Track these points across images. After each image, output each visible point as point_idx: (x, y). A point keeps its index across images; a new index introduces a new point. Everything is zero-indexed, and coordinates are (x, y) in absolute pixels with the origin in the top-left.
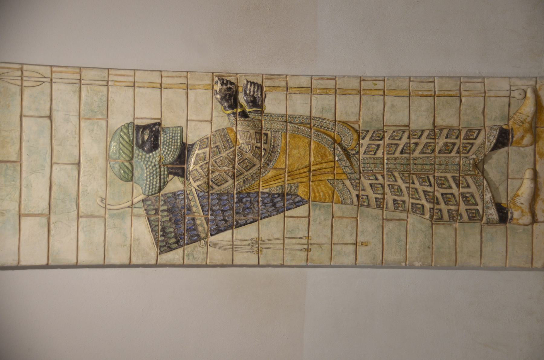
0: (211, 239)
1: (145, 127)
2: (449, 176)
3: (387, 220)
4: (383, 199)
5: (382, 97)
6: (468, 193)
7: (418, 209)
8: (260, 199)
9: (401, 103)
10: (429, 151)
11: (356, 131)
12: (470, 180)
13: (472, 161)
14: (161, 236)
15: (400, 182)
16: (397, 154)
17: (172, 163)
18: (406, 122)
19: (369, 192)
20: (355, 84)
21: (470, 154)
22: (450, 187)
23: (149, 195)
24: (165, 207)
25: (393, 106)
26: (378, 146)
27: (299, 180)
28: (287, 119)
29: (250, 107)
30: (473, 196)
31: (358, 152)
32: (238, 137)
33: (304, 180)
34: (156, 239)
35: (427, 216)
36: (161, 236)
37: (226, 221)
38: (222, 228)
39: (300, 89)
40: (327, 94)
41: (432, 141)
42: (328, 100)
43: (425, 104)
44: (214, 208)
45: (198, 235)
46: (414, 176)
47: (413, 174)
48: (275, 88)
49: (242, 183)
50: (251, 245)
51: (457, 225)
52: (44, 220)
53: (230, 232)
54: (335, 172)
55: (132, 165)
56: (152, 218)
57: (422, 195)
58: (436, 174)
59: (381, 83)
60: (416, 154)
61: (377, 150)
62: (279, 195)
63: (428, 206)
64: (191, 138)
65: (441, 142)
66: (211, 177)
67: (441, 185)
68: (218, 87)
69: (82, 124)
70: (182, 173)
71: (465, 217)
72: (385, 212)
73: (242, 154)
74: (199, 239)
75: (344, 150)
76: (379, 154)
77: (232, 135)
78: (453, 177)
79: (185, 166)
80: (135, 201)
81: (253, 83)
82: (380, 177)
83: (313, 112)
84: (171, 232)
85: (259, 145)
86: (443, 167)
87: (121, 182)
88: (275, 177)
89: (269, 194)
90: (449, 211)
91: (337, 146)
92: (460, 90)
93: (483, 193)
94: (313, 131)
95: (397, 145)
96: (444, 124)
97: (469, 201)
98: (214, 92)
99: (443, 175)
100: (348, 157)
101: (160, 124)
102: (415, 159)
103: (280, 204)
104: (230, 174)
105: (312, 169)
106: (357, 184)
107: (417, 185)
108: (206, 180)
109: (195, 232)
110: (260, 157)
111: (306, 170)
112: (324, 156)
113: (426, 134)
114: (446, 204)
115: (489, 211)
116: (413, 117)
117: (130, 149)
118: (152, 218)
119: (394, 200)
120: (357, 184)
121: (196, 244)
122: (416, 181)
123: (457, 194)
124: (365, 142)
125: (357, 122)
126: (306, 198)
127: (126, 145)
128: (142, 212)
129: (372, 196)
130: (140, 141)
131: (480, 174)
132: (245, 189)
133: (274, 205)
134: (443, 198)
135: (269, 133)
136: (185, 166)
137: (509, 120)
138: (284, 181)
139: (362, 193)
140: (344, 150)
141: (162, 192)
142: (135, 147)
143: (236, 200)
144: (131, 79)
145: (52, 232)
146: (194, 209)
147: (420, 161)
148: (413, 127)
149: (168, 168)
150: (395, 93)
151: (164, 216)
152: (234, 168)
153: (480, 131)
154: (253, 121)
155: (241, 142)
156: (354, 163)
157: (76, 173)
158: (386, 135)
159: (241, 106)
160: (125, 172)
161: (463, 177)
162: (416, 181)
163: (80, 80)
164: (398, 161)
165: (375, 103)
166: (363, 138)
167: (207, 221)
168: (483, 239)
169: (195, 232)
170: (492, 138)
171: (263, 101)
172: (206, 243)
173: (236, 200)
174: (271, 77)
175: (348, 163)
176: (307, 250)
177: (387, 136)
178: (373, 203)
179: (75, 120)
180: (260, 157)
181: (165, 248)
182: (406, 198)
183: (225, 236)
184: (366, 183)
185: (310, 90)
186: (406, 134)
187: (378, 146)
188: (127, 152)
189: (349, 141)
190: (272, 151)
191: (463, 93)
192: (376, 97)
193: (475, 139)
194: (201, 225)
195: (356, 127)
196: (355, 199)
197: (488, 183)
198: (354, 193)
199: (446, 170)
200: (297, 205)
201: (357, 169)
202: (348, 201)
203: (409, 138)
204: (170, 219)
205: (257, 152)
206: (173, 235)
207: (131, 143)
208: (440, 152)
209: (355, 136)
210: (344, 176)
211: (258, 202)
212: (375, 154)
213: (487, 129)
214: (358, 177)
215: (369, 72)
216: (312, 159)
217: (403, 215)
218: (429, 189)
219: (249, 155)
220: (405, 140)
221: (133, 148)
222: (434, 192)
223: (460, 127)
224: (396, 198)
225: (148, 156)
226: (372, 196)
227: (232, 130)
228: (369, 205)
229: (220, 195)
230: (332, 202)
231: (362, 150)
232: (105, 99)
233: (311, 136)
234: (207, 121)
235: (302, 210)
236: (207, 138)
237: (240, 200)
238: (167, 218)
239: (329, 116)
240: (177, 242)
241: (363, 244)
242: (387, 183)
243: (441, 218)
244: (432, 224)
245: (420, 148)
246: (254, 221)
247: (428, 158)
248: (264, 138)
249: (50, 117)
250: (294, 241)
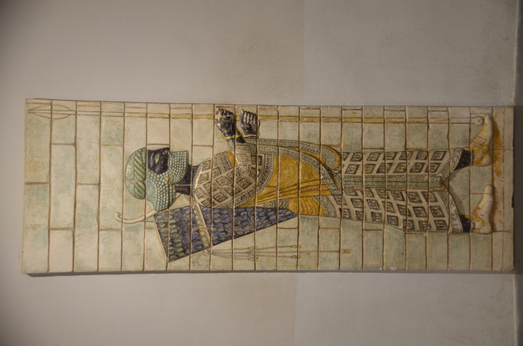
0: (214, 248)
1: (156, 152)
2: (419, 191)
3: (366, 230)
4: (363, 212)
5: (360, 124)
6: (436, 206)
7: (393, 221)
8: (256, 213)
9: (377, 129)
10: (402, 170)
11: (338, 153)
12: (438, 196)
13: (439, 179)
14: (171, 246)
15: (377, 197)
16: (374, 173)
17: (179, 183)
18: (381, 145)
19: (350, 206)
20: (336, 113)
21: (437, 172)
22: (420, 201)
23: (159, 211)
24: (174, 221)
25: (370, 131)
26: (358, 166)
27: (289, 196)
28: (279, 144)
29: (247, 134)
30: (440, 209)
31: (340, 172)
32: (236, 159)
33: (294, 196)
34: (166, 249)
35: (401, 227)
36: (171, 246)
37: (226, 233)
38: (223, 239)
39: (290, 118)
40: (313, 121)
41: (404, 161)
42: (314, 127)
43: (398, 129)
44: (216, 221)
45: (202, 245)
46: (389, 192)
47: (388, 190)
48: (268, 117)
49: (240, 200)
50: (248, 253)
51: (427, 234)
52: (70, 233)
53: (230, 241)
54: (321, 189)
55: (145, 185)
56: (162, 231)
57: (396, 208)
58: (408, 190)
59: (360, 112)
60: (391, 173)
61: (357, 169)
62: (272, 209)
63: (401, 218)
64: (195, 161)
65: (412, 162)
66: (213, 194)
67: (412, 200)
68: (219, 116)
69: (102, 150)
70: (188, 191)
71: (434, 227)
72: (364, 224)
73: (239, 174)
74: (203, 248)
75: (328, 169)
76: (359, 173)
77: (231, 158)
78: (423, 193)
79: (191, 185)
80: (148, 215)
82: (359, 193)
83: (301, 137)
84: (179, 243)
85: (254, 166)
86: (414, 184)
87: (136, 199)
88: (269, 194)
89: (263, 208)
90: (420, 222)
91: (322, 167)
92: (427, 117)
93: (448, 206)
94: (301, 153)
95: (374, 165)
96: (414, 147)
97: (437, 213)
98: (215, 121)
99: (414, 191)
100: (332, 176)
101: (168, 149)
102: (390, 177)
103: (273, 217)
104: (230, 191)
105: (301, 186)
106: (340, 199)
107: (392, 200)
108: (208, 196)
109: (199, 243)
110: (255, 176)
111: (295, 187)
112: (310, 175)
113: (399, 155)
114: (417, 216)
115: (454, 222)
116: (387, 141)
117: (143, 171)
118: (162, 231)
119: (372, 213)
120: (340, 199)
121: (201, 252)
122: (391, 196)
123: (426, 207)
124: (346, 163)
125: (339, 145)
126: (296, 212)
127: (140, 168)
128: (154, 225)
129: (353, 210)
130: (152, 164)
131: (446, 190)
132: (242, 205)
133: (268, 218)
134: (415, 211)
135: (263, 155)
136: (191, 185)
137: (470, 143)
138: (276, 197)
139: (345, 207)
140: (328, 169)
141: (171, 208)
142: (147, 169)
143: (234, 214)
144: (144, 111)
145: (77, 244)
146: (199, 222)
147: (394, 179)
148: (387, 149)
149: (176, 187)
150: (372, 120)
151: (172, 229)
152: (233, 186)
153: (445, 152)
154: (249, 145)
155: (239, 163)
156: (337, 181)
157: (97, 192)
158: (364, 156)
159: (239, 133)
160: (139, 191)
161: (431, 192)
162: (391, 196)
163: (101, 112)
164: (375, 179)
165: (354, 129)
166: (345, 160)
167: (210, 232)
168: (450, 246)
169: (199, 243)
170: (455, 158)
171: (257, 129)
172: (209, 251)
173: (234, 214)
174: (264, 107)
175: (332, 182)
176: (297, 257)
177: (365, 157)
178: (354, 215)
179: (96, 146)
180: (255, 176)
181: (174, 256)
182: (382, 211)
183: (226, 246)
184: (348, 198)
185: (298, 118)
186: (382, 156)
187: (358, 166)
188: (141, 174)
189: (332, 161)
190: (266, 171)
191: (430, 120)
192: (356, 124)
193: (441, 160)
194: (205, 236)
195: (338, 149)
196: (338, 213)
197: (453, 198)
198: (337, 207)
199: (417, 187)
200: (287, 217)
201: (339, 186)
202: (332, 214)
203: (384, 159)
204: (178, 231)
205: (253, 172)
206: (180, 245)
207: (144, 166)
208: (411, 171)
209: (338, 158)
210: (328, 193)
211: (254, 215)
212: (355, 173)
213: (451, 150)
214: (340, 193)
215: (349, 102)
216: (301, 178)
217: (380, 226)
218: (402, 203)
219: (246, 175)
220: (380, 161)
221: (145, 169)
222: (406, 206)
223: (428, 149)
224: (374, 211)
225: (158, 176)
226: (353, 210)
227: (231, 154)
228: (350, 218)
229: (221, 209)
230: (319, 215)
231: (344, 170)
232: (122, 128)
233: (299, 158)
234: (209, 146)
235: (292, 223)
236: (210, 161)
237: (238, 214)
238: (176, 231)
239: (315, 141)
240: (184, 251)
241: (345, 251)
242: (365, 198)
243: (413, 228)
244: (405, 233)
245: (394, 167)
246: (251, 232)
247: (401, 176)
248: (259, 160)
249: (75, 144)
250: (285, 249)
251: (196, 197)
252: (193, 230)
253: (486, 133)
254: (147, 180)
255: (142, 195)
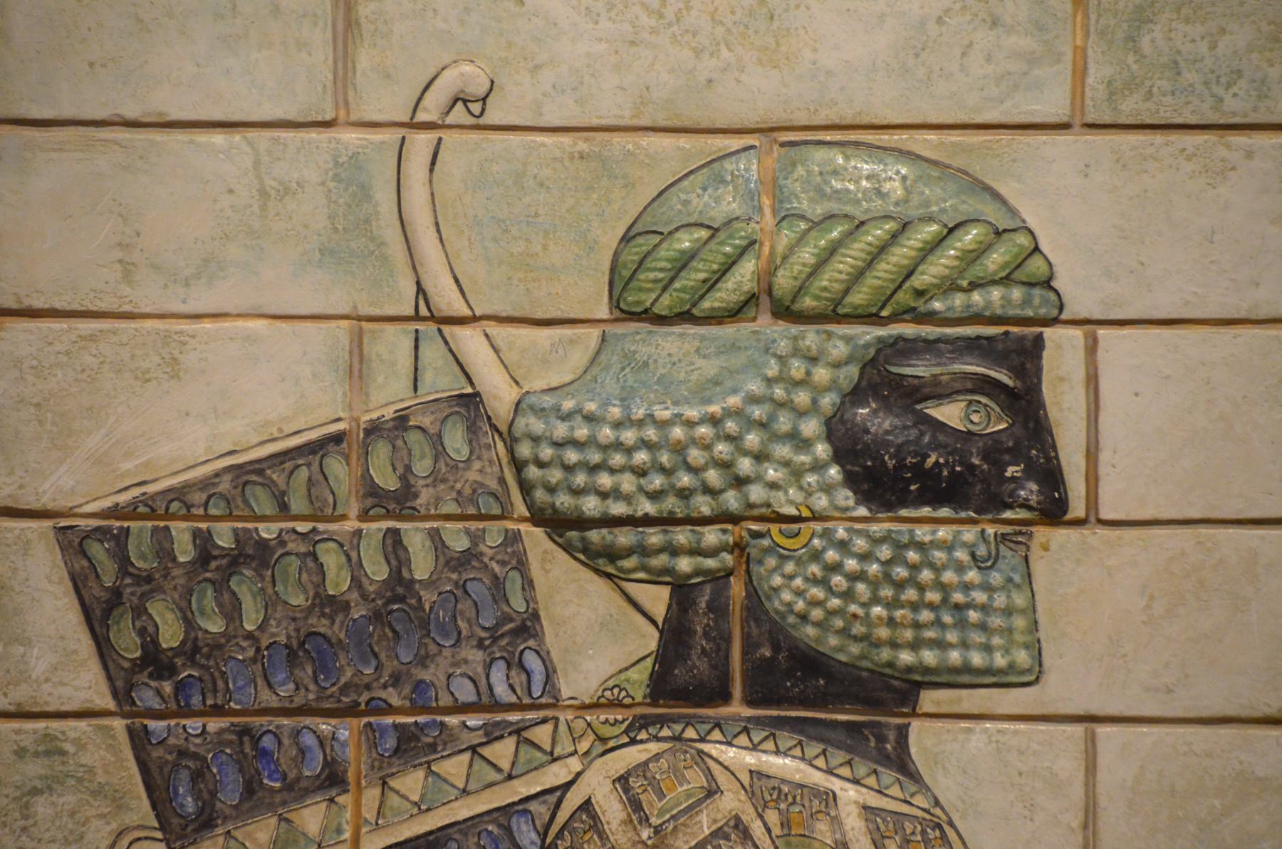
14: (203, 541)
17: (755, 603)
23: (511, 441)
24: (422, 565)
36: (203, 541)
55: (734, 314)
56: (337, 467)
79: (738, 708)
80: (470, 341)
84: (233, 612)
117: (859, 297)
118: (337, 467)
127: (885, 269)
130: (920, 369)
136: (738, 708)
141: (536, 539)
142: (869, 334)
160: (684, 262)
204: (336, 605)
206: (215, 626)
221: (870, 317)
225: (811, 427)
238: (338, 581)
251: (633, 755)
252: (346, 730)
254: (780, 333)
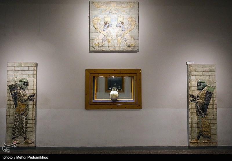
11: (27, 116)
28: (28, 105)
70: (20, 89)
76: (23, 119)
81: (34, 99)
88: (19, 103)
100: (22, 114)
106: (18, 116)
112: (22, 110)
120: (18, 116)
124: (25, 117)
129: (16, 118)
148: (27, 124)
184: (18, 117)
189: (25, 114)
205: (22, 100)
220: (25, 123)
226: (16, 118)
235: (15, 107)
249: (29, 70)
253: (30, 142)
255: (20, 81)
